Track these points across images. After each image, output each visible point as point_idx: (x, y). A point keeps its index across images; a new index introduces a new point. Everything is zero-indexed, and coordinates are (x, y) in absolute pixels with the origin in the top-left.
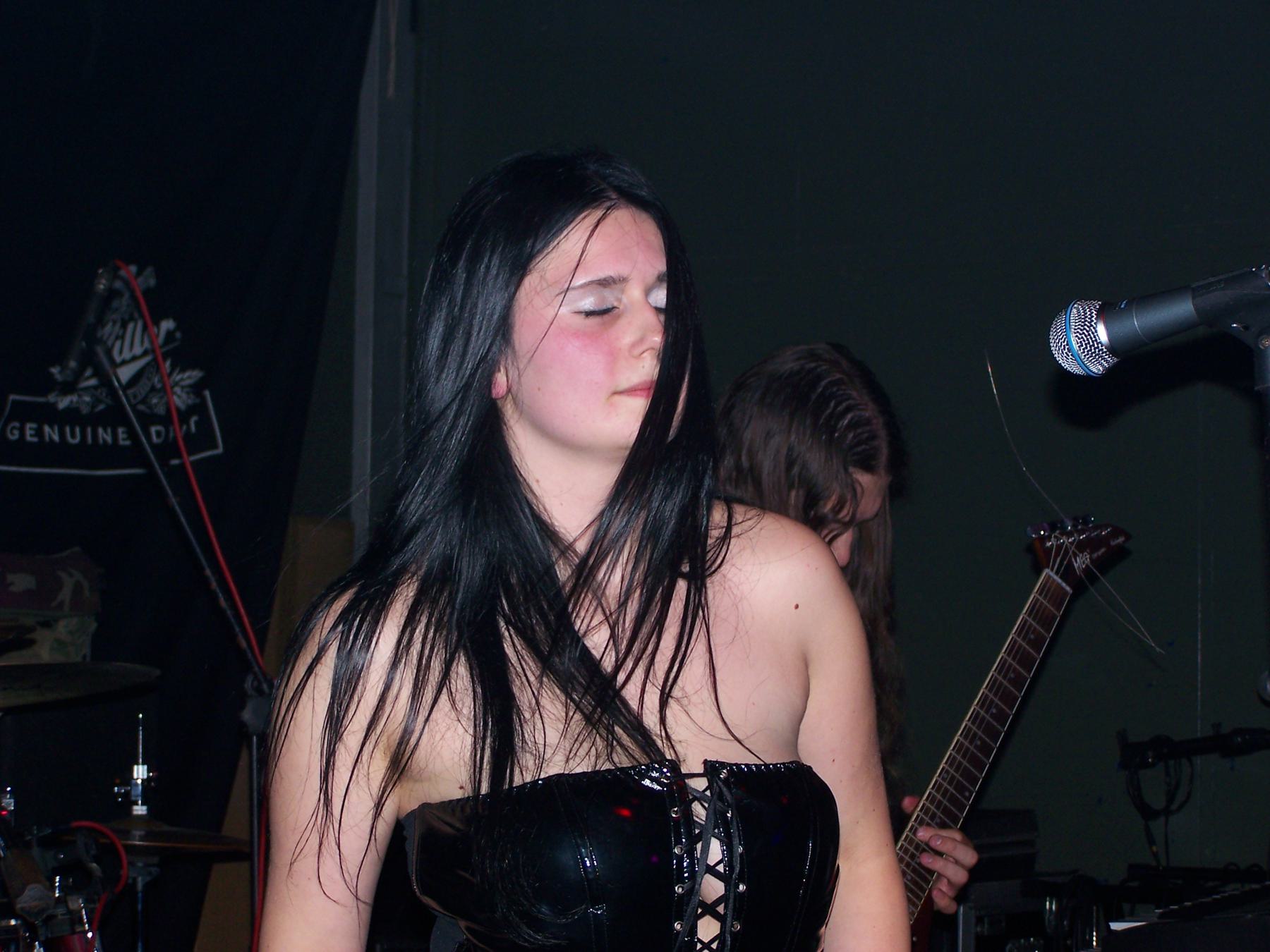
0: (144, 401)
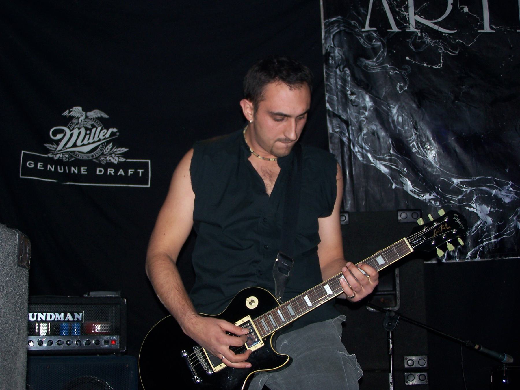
0: (96, 158)
